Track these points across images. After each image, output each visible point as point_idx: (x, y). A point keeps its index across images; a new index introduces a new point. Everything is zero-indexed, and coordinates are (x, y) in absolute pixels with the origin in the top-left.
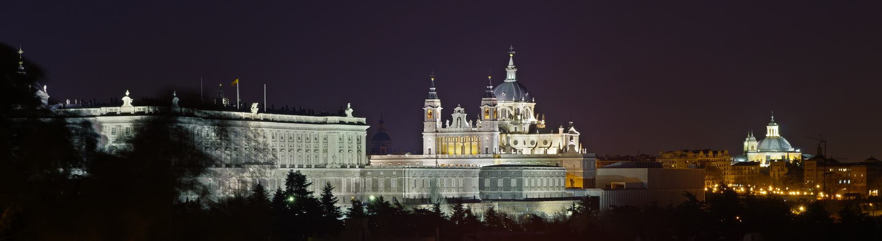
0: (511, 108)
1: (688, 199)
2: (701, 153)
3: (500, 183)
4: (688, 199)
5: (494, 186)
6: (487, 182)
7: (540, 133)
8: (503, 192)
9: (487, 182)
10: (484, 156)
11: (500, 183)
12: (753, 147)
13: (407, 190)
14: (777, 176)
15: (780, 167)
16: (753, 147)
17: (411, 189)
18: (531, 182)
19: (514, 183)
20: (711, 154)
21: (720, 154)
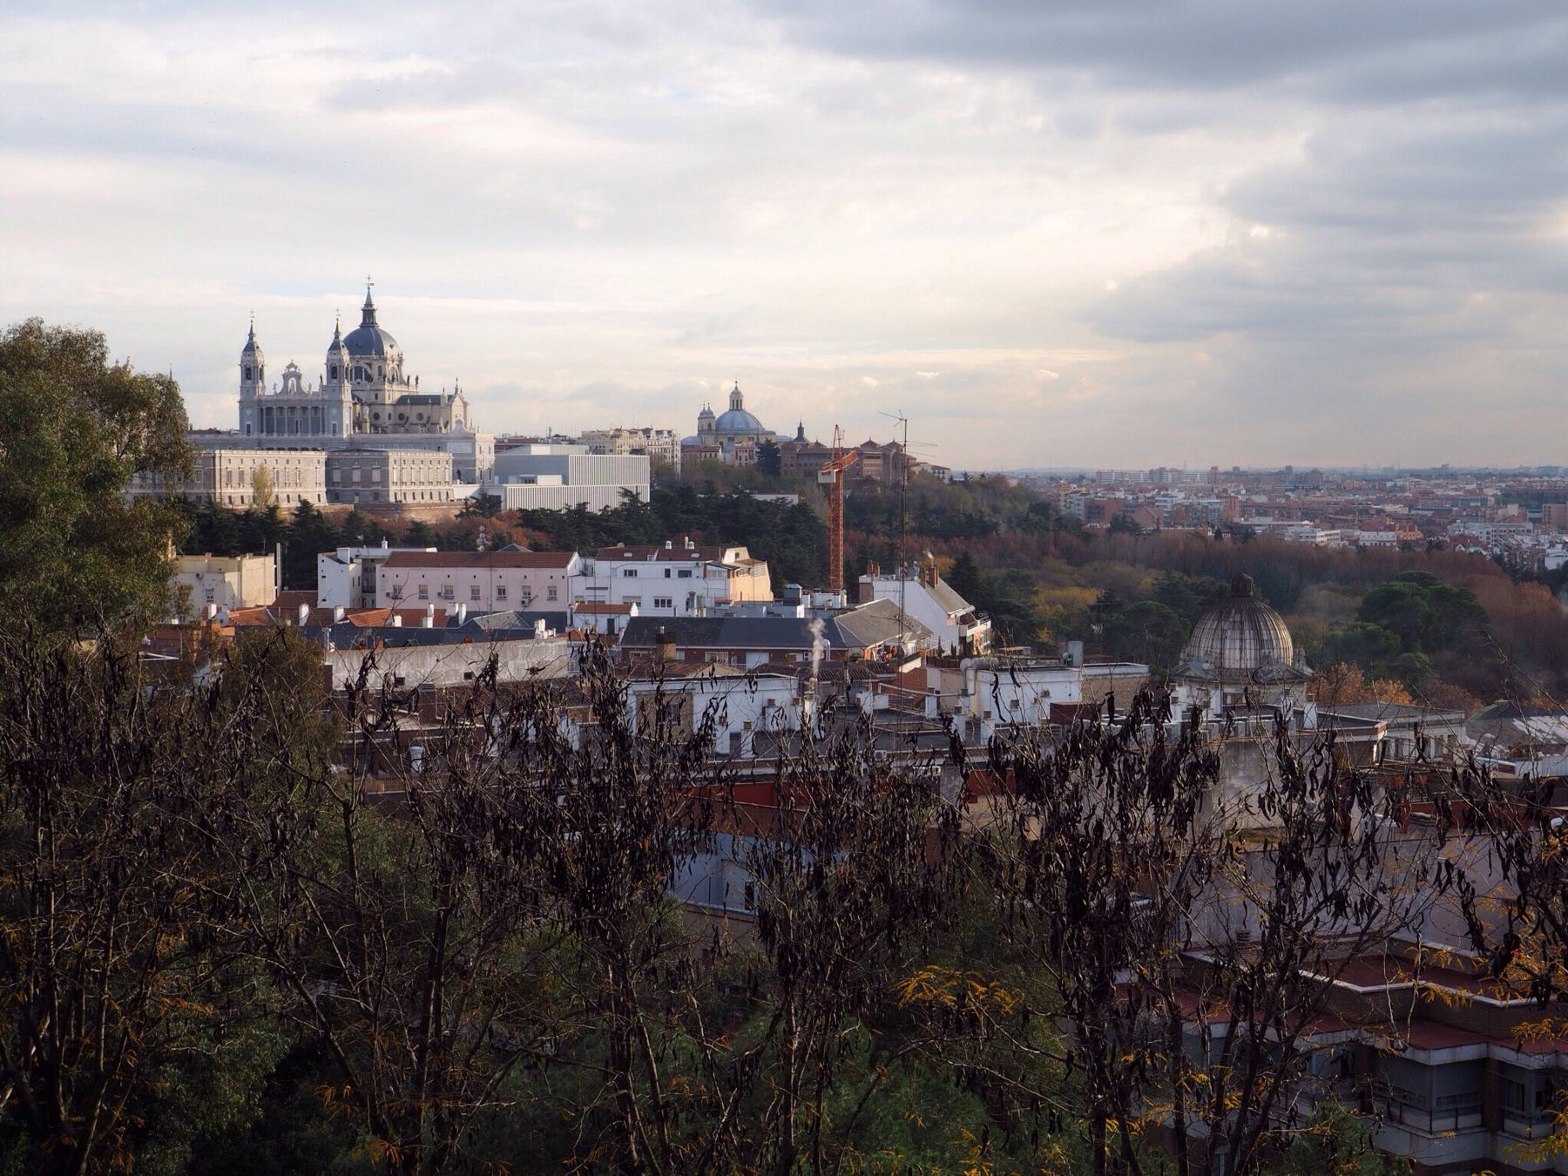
0: (370, 365)
1: (626, 500)
2: (640, 433)
3: (356, 476)
4: (626, 500)
5: (347, 479)
6: (337, 477)
7: (412, 404)
8: (360, 488)
9: (337, 477)
10: (331, 436)
11: (356, 476)
12: (710, 425)
13: (218, 486)
14: (743, 464)
15: (747, 454)
16: (710, 425)
17: (224, 484)
18: (401, 474)
19: (376, 476)
20: (653, 433)
21: (666, 434)
